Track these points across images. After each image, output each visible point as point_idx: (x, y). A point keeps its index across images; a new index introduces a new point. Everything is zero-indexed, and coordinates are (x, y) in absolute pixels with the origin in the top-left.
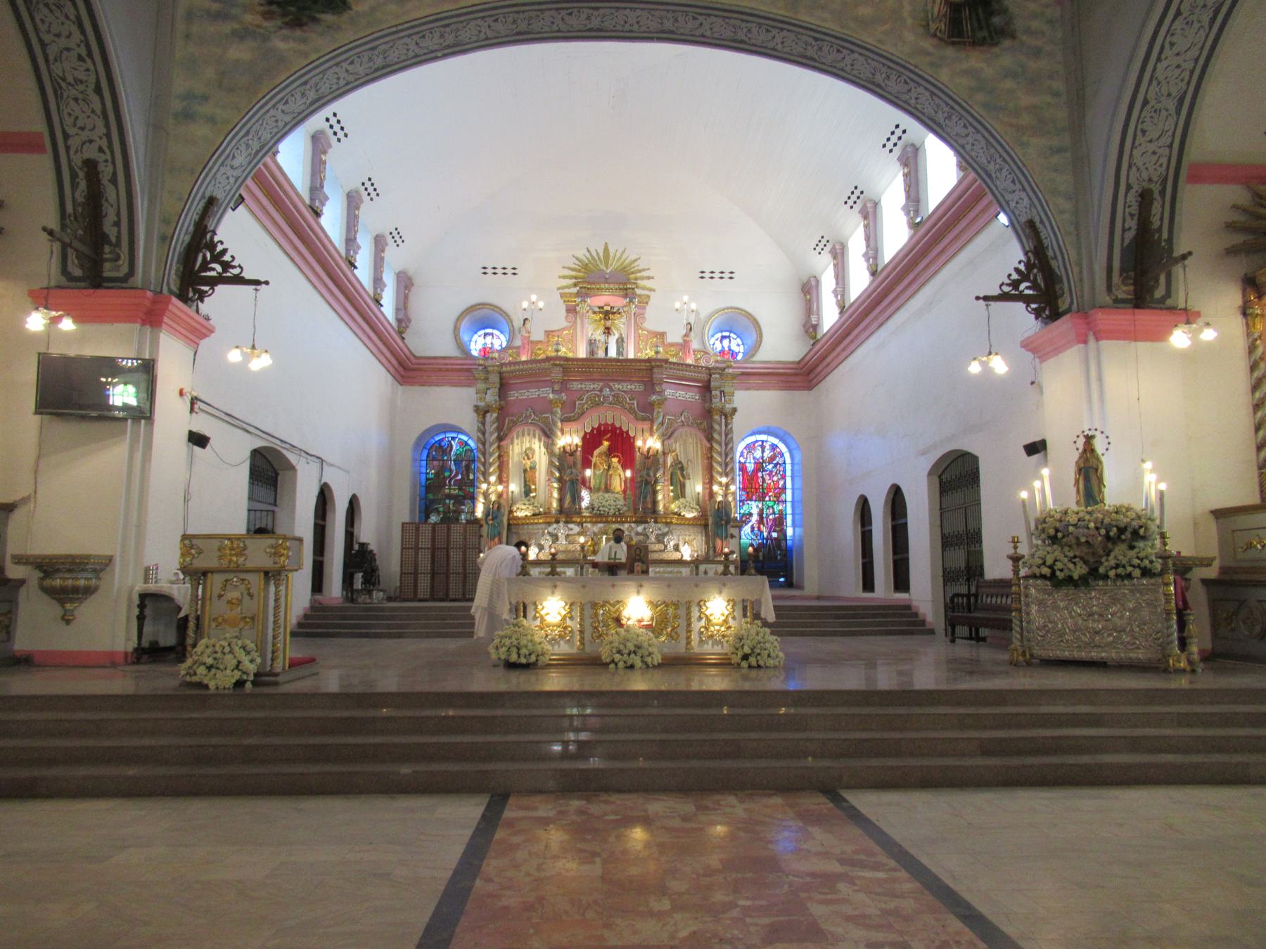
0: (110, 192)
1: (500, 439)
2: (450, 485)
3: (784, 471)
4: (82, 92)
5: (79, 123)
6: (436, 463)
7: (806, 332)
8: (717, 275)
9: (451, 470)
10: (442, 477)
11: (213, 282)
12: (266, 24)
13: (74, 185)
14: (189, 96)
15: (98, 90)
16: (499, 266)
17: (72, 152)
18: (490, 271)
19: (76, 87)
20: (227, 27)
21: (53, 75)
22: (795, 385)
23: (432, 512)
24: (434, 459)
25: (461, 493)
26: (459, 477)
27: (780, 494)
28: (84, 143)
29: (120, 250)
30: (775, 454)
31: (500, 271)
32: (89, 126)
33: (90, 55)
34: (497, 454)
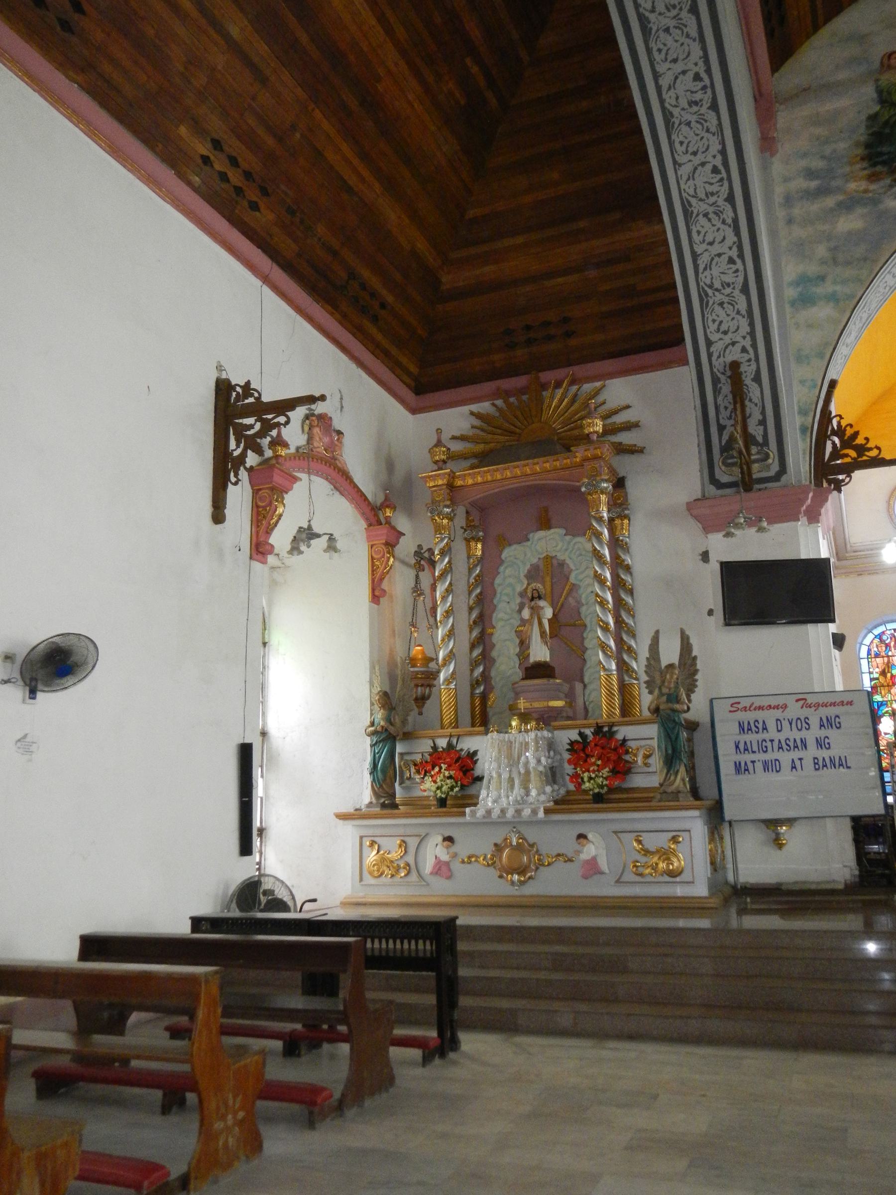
0: (754, 392)
4: (728, 295)
5: (724, 327)
6: (879, 660)
10: (889, 675)
11: (848, 469)
12: (873, 187)
13: (716, 391)
14: (803, 280)
15: (745, 290)
17: (714, 358)
19: (723, 291)
20: (830, 202)
21: (702, 284)
24: (877, 656)
28: (726, 347)
29: (768, 449)
32: (732, 329)
33: (741, 256)
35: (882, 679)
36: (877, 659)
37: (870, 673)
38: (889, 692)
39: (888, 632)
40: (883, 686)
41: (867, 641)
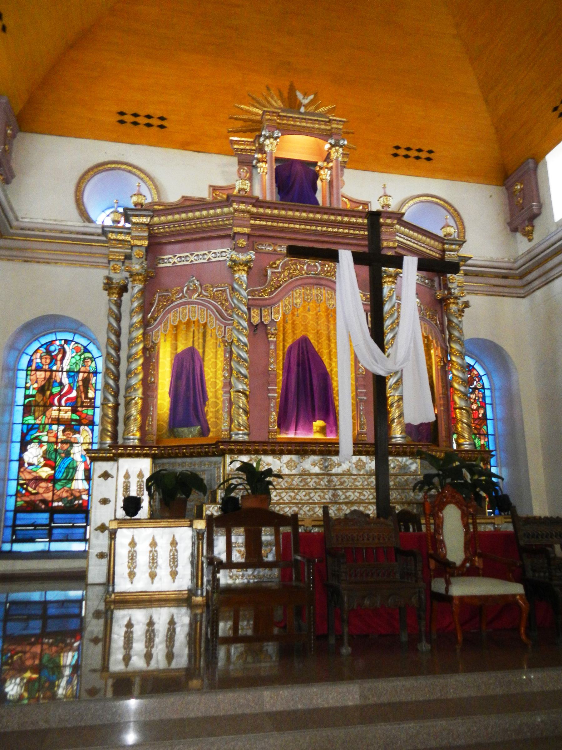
1: (145, 324)
2: (60, 405)
3: (484, 397)
6: (41, 375)
7: (514, 230)
8: (413, 153)
9: (61, 384)
10: (48, 393)
16: (142, 113)
18: (129, 118)
22: (506, 290)
23: (31, 442)
24: (38, 369)
25: (75, 417)
26: (74, 394)
27: (480, 425)
30: (471, 376)
31: (142, 120)
34: (141, 346)
35: (39, 398)
36: (38, 373)
37: (26, 388)
38: (44, 413)
39: (58, 343)
40: (37, 405)
41: (31, 350)
